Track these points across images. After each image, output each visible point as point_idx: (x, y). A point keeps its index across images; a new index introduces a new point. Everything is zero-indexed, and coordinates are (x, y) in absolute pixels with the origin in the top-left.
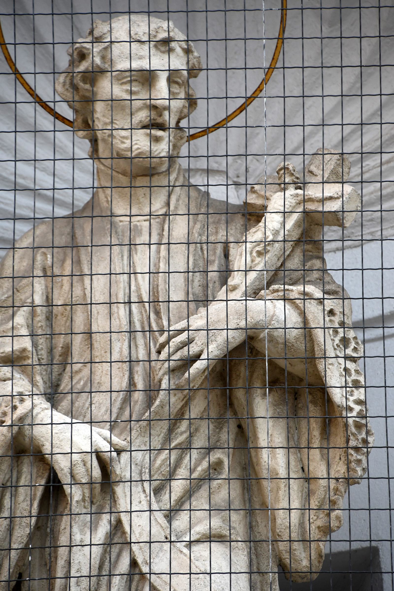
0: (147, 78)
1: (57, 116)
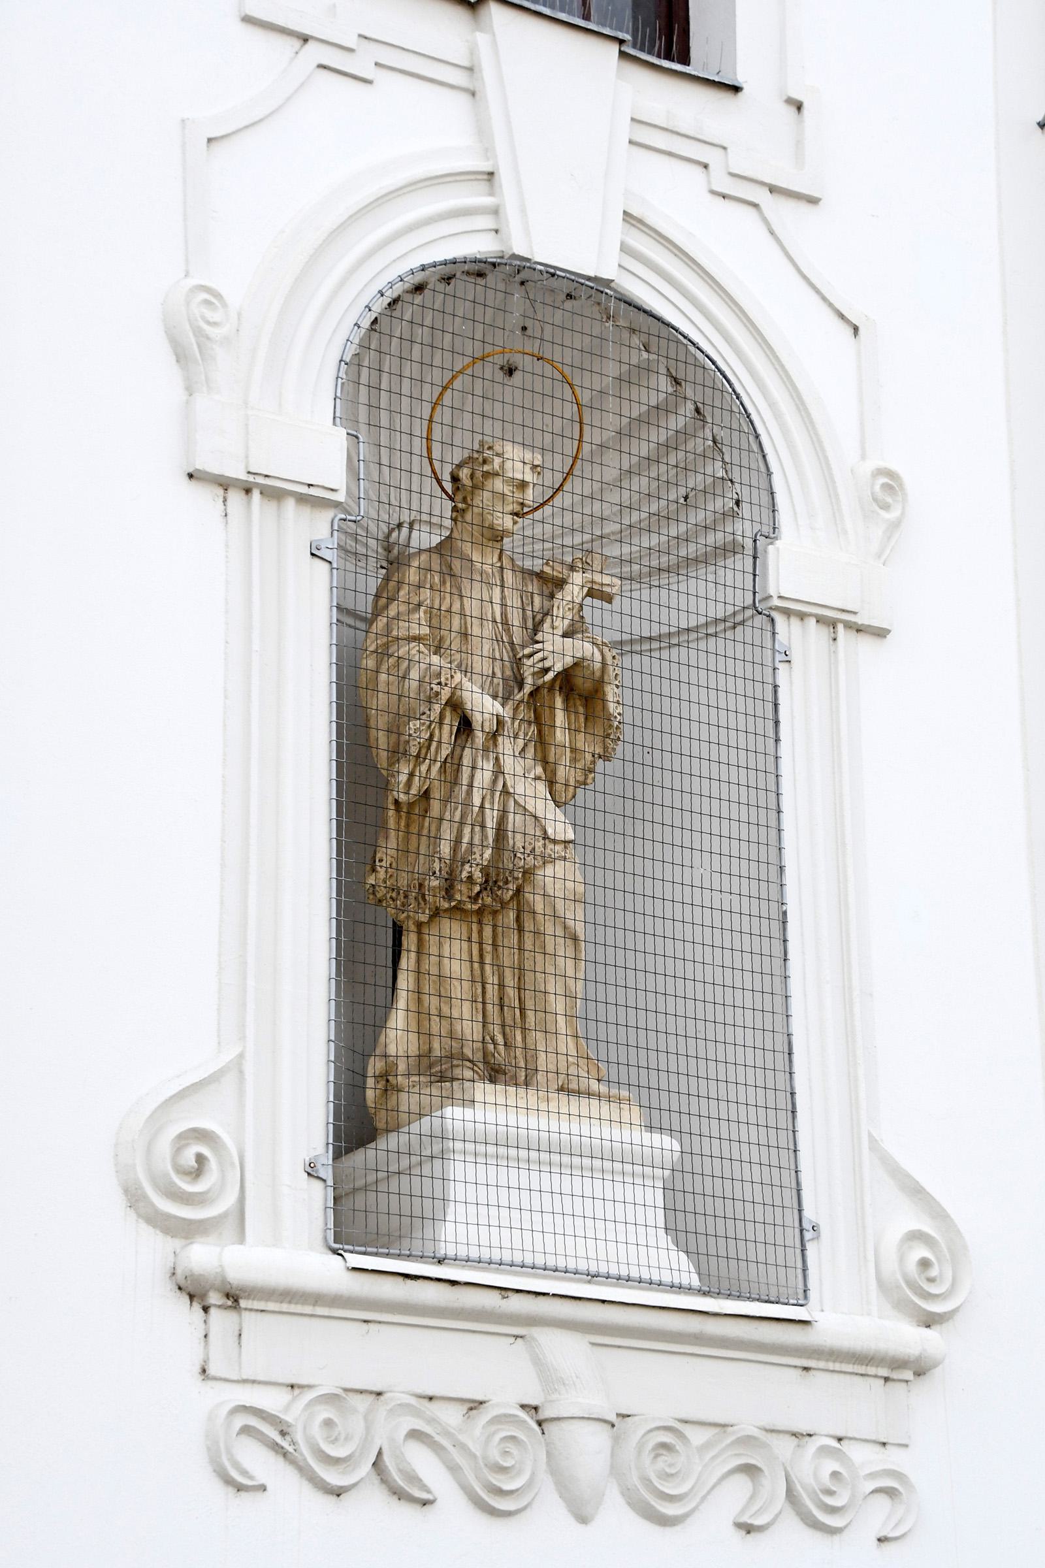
0: (523, 485)
1: (443, 489)
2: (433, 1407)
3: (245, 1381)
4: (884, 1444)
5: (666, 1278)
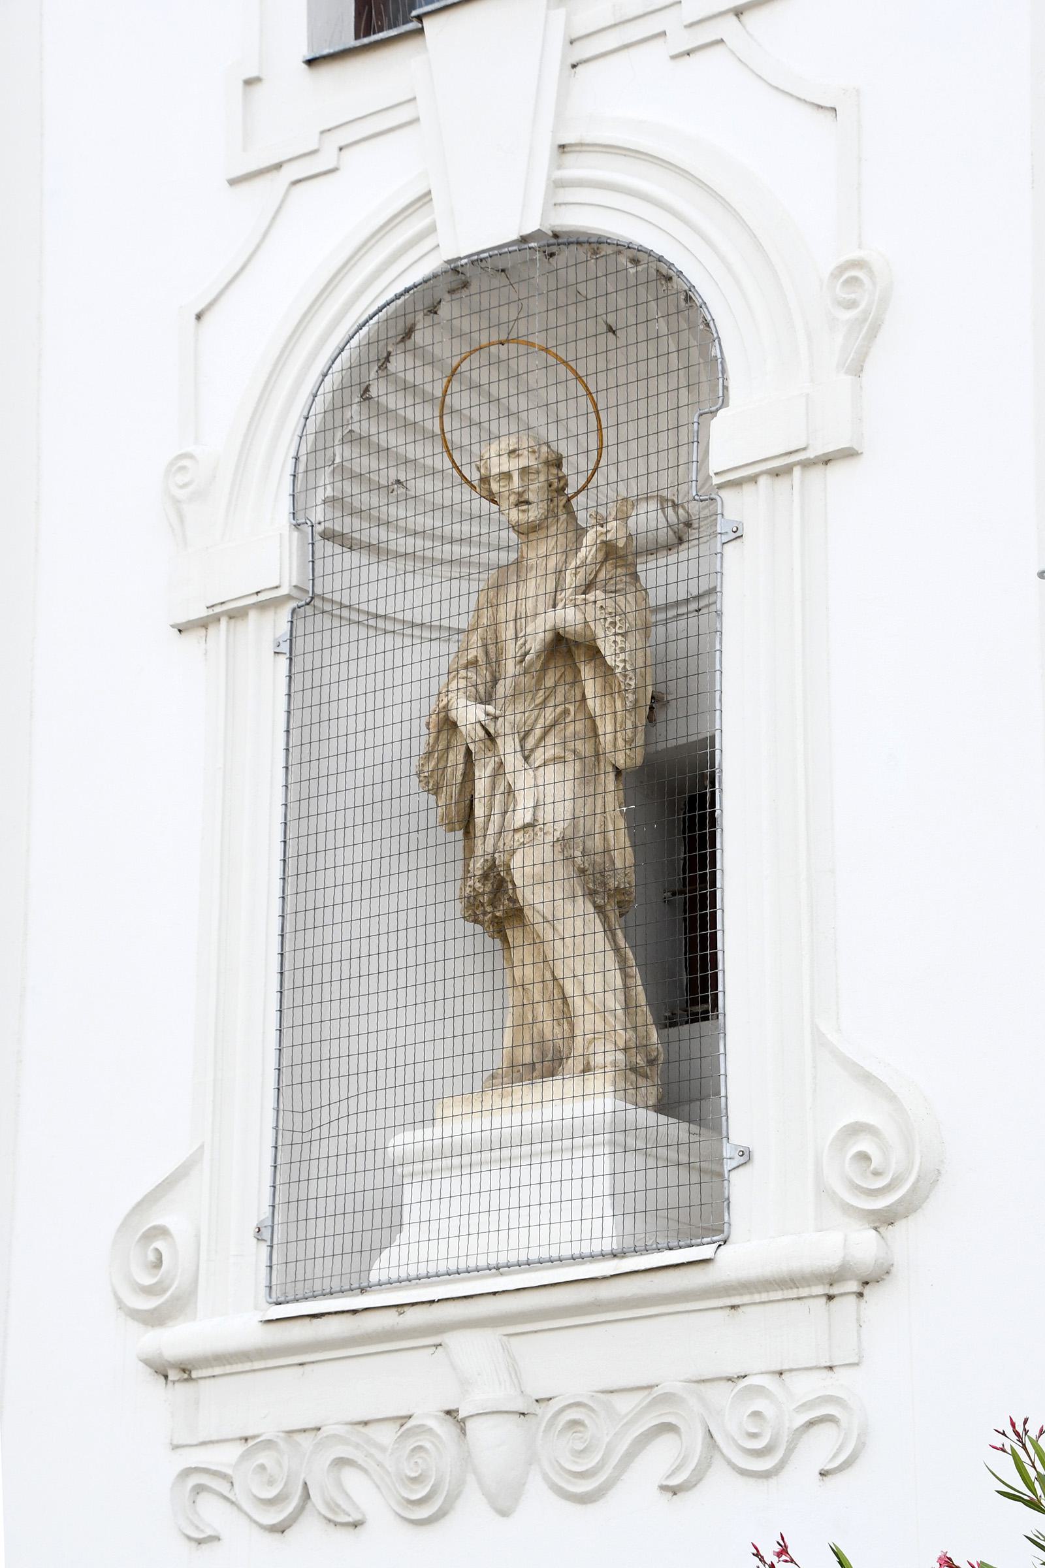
0: (508, 475)
2: (369, 1430)
3: (203, 1443)
4: (831, 1368)
5: (566, 1252)
